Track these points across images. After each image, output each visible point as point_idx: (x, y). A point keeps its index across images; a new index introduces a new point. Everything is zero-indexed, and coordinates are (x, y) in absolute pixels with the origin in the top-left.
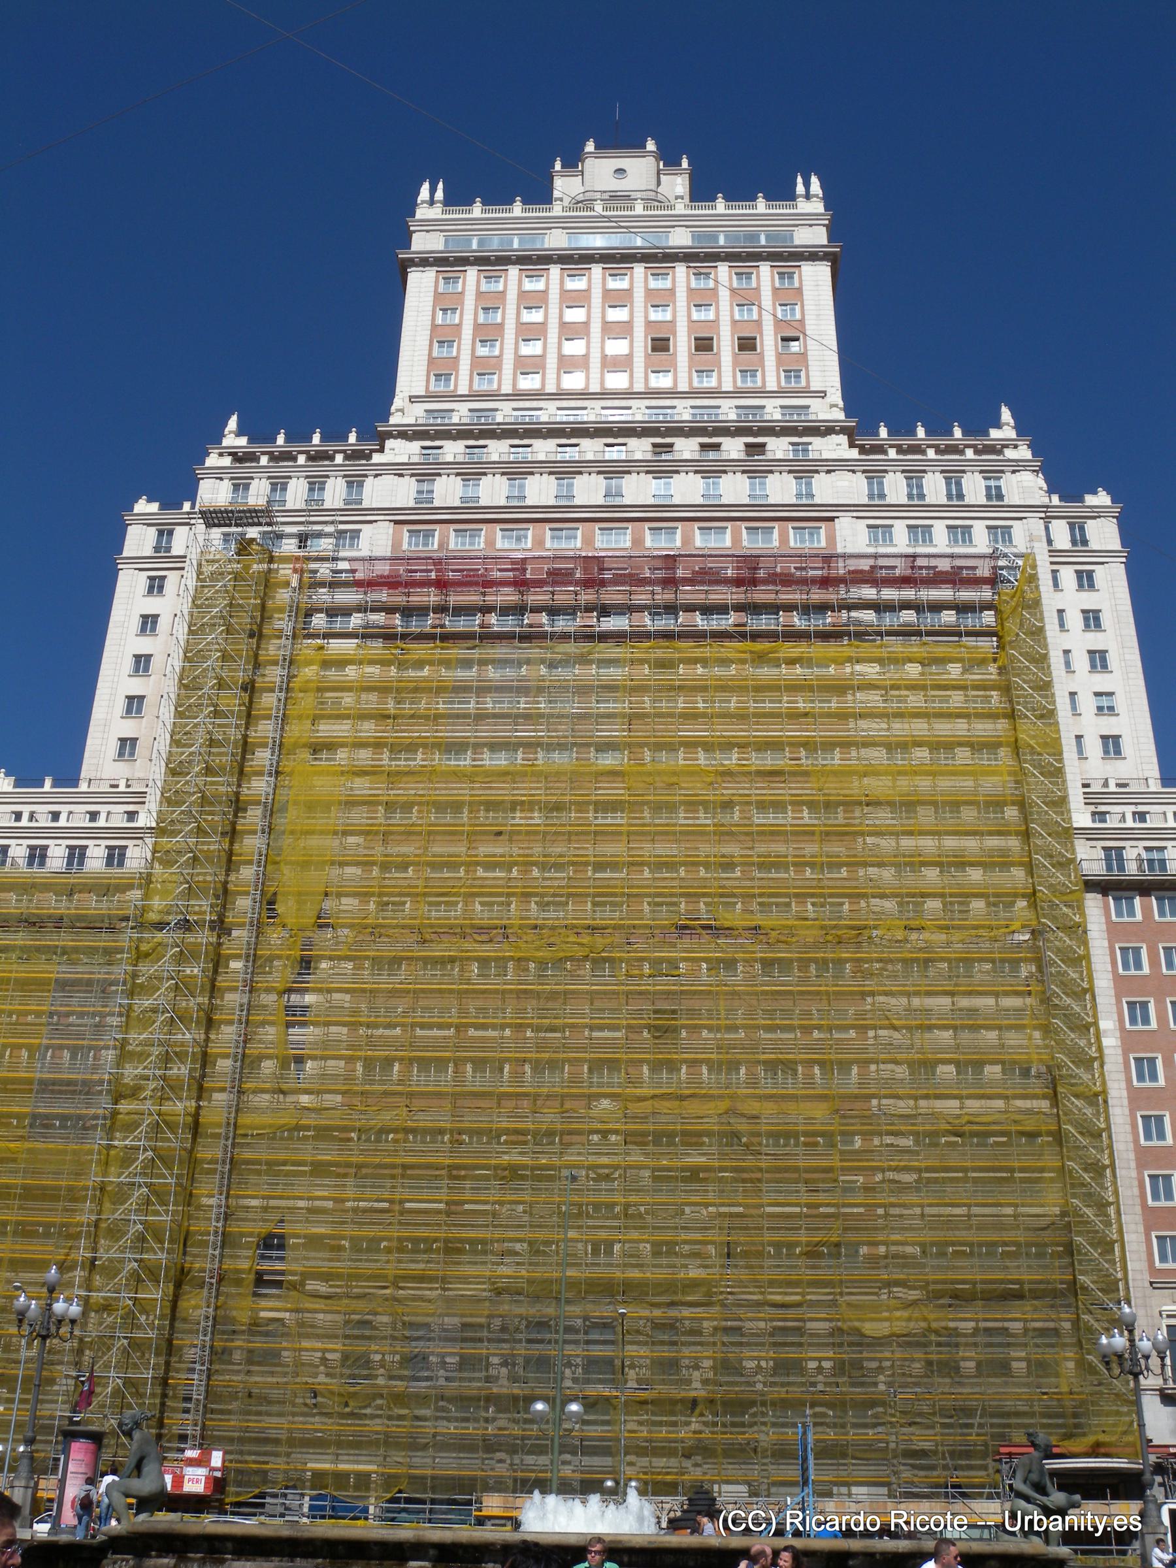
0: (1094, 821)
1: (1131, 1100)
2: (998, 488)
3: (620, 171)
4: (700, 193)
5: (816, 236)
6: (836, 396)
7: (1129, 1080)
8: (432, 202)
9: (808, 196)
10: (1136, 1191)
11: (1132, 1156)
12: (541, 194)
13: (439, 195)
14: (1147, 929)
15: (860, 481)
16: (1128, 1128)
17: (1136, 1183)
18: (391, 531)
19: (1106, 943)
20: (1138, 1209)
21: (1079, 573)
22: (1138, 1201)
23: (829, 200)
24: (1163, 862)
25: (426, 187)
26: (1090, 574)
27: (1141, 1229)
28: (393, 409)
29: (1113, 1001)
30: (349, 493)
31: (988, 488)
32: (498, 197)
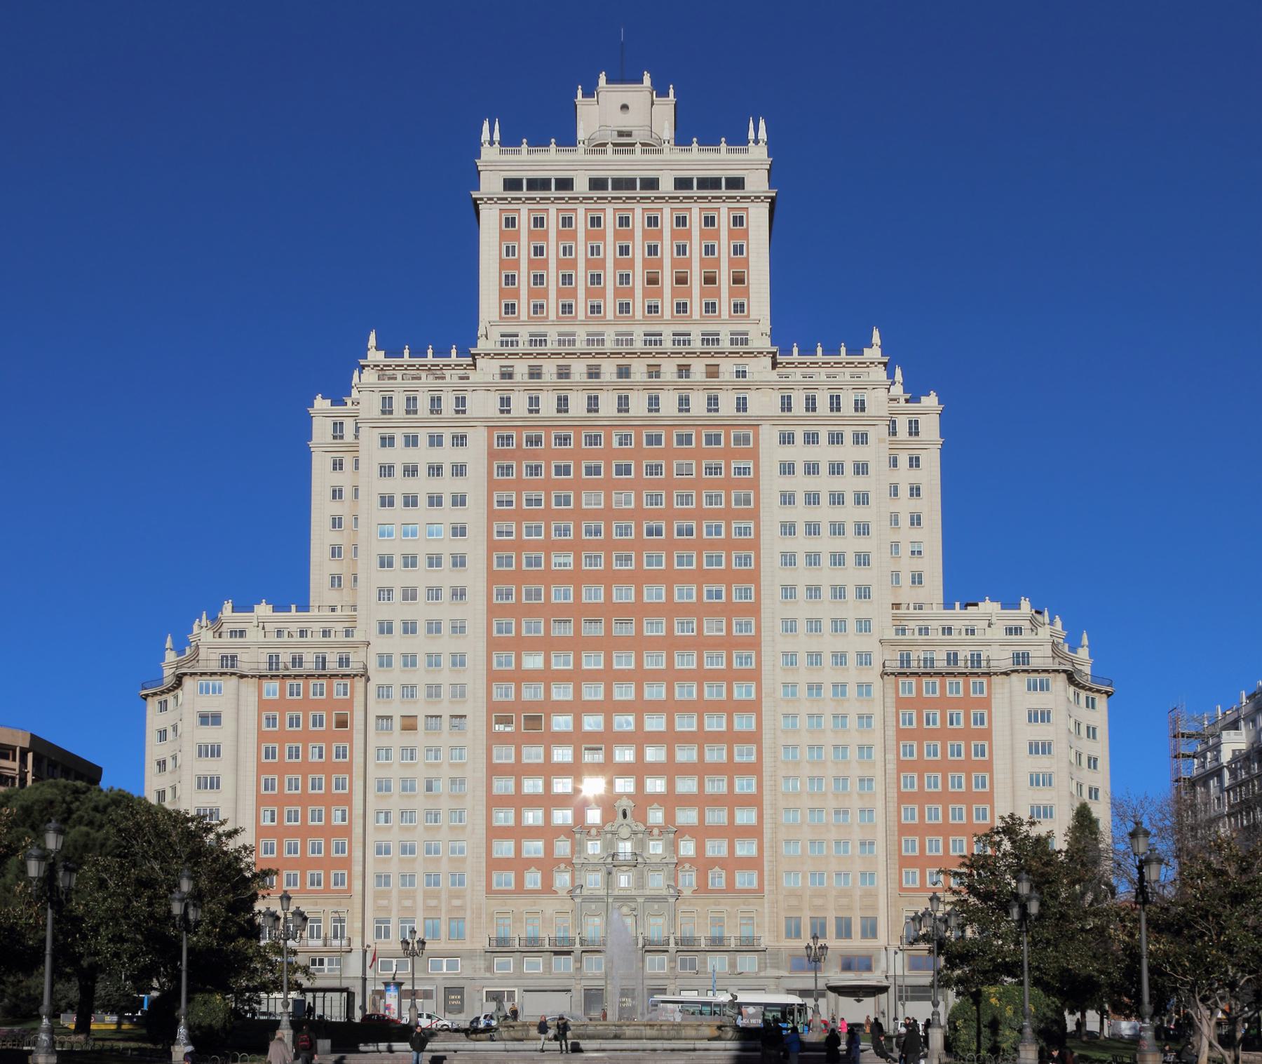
0: (897, 634)
1: (899, 798)
2: (863, 402)
4: (682, 139)
5: (758, 182)
6: (766, 326)
8: (492, 143)
9: (756, 142)
10: (897, 848)
11: (896, 829)
12: (568, 139)
13: (497, 136)
14: (919, 703)
15: (776, 398)
16: (896, 813)
17: (896, 843)
18: (486, 434)
19: (894, 710)
20: (897, 857)
22: (897, 852)
23: (768, 143)
24: (932, 660)
25: (486, 126)
27: (897, 867)
28: (481, 331)
29: (895, 743)
30: (457, 405)
31: (856, 401)
32: (539, 141)
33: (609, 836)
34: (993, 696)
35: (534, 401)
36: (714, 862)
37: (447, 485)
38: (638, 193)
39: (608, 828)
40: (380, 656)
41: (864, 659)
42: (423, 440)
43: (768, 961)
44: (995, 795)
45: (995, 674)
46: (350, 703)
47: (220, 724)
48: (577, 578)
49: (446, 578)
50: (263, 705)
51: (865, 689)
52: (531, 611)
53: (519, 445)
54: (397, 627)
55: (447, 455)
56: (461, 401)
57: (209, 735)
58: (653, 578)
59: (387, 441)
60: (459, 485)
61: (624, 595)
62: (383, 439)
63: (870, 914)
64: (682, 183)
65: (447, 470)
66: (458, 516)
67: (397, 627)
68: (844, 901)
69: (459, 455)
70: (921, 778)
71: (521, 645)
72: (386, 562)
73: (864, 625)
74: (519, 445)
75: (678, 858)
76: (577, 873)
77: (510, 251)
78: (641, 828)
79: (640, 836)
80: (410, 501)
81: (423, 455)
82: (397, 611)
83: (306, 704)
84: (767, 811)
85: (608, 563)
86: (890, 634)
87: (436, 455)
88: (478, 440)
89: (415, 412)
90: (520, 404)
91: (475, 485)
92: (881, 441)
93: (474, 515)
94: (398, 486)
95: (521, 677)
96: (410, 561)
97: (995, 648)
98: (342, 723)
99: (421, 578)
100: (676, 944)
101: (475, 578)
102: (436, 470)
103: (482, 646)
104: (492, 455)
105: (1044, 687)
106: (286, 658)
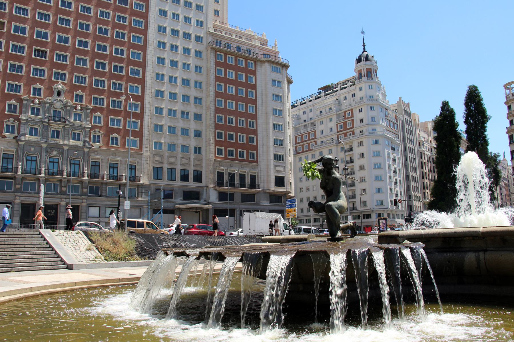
7: (215, 105)
20: (214, 140)
34: (257, 70)
36: (113, 130)
41: (199, 39)
43: (143, 191)
44: (258, 116)
51: (198, 54)
63: (198, 169)
68: (185, 161)
70: (226, 102)
73: (199, 23)
75: (91, 125)
76: (21, 125)
84: (147, 106)
86: (212, 30)
100: (88, 177)
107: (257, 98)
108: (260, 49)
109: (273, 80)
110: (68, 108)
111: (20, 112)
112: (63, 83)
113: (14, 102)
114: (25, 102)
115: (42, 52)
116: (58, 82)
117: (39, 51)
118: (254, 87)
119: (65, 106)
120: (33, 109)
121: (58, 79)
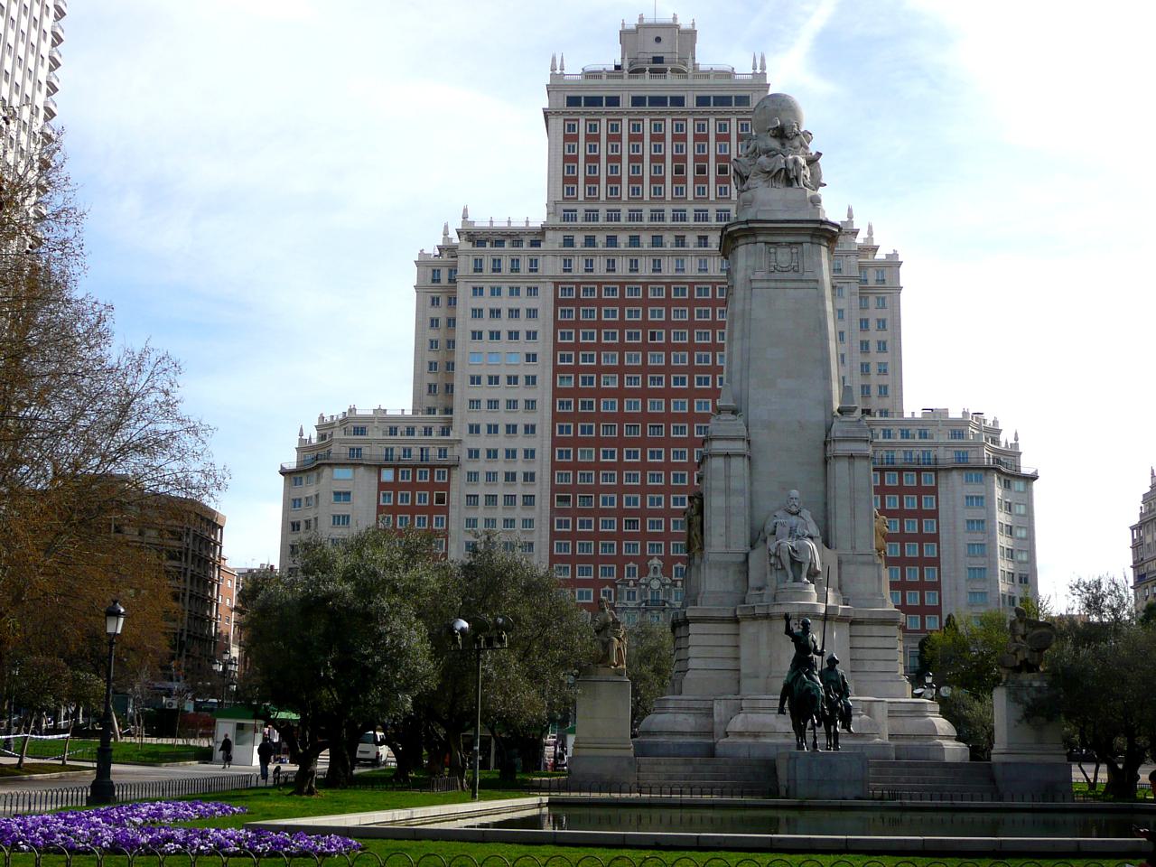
3: (658, 40)
21: (878, 298)
24: (893, 458)
26: (883, 299)
33: (643, 587)
35: (589, 263)
37: (522, 325)
38: (669, 108)
39: (642, 581)
40: (470, 451)
42: (505, 290)
44: (941, 560)
45: (940, 469)
46: (447, 486)
47: (349, 500)
48: (620, 393)
49: (521, 393)
50: (382, 486)
52: (585, 417)
53: (578, 295)
54: (484, 429)
55: (523, 302)
56: (534, 263)
57: (342, 509)
58: (679, 394)
59: (478, 291)
60: (532, 325)
61: (656, 406)
62: (475, 289)
64: (702, 101)
65: (523, 313)
66: (531, 347)
67: (484, 429)
69: (533, 303)
71: (577, 442)
72: (475, 380)
74: (578, 295)
77: (572, 148)
78: (668, 581)
79: (667, 587)
80: (495, 335)
81: (505, 303)
82: (483, 418)
83: (414, 486)
85: (645, 383)
87: (514, 303)
88: (547, 292)
89: (499, 270)
90: (578, 267)
91: (544, 325)
92: (852, 294)
93: (543, 347)
94: (486, 325)
95: (576, 466)
96: (494, 380)
97: (941, 449)
98: (441, 499)
99: (502, 393)
101: (543, 394)
102: (514, 313)
103: (548, 443)
104: (558, 302)
105: (979, 481)
106: (398, 452)
107: (940, 531)
108: (947, 446)
109: (967, 497)
110: (667, 587)
111: (615, 599)
112: (659, 558)
113: (607, 588)
114: (619, 586)
115: (634, 521)
116: (652, 557)
117: (630, 521)
118: (934, 514)
119: (664, 585)
120: (629, 592)
121: (653, 552)
